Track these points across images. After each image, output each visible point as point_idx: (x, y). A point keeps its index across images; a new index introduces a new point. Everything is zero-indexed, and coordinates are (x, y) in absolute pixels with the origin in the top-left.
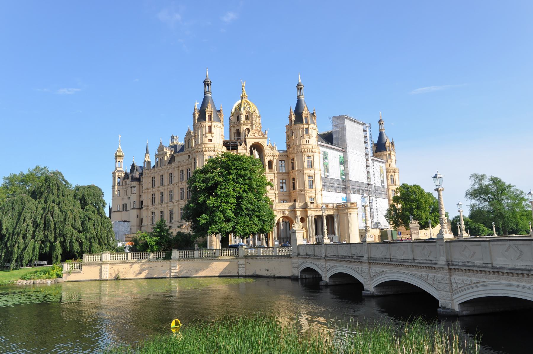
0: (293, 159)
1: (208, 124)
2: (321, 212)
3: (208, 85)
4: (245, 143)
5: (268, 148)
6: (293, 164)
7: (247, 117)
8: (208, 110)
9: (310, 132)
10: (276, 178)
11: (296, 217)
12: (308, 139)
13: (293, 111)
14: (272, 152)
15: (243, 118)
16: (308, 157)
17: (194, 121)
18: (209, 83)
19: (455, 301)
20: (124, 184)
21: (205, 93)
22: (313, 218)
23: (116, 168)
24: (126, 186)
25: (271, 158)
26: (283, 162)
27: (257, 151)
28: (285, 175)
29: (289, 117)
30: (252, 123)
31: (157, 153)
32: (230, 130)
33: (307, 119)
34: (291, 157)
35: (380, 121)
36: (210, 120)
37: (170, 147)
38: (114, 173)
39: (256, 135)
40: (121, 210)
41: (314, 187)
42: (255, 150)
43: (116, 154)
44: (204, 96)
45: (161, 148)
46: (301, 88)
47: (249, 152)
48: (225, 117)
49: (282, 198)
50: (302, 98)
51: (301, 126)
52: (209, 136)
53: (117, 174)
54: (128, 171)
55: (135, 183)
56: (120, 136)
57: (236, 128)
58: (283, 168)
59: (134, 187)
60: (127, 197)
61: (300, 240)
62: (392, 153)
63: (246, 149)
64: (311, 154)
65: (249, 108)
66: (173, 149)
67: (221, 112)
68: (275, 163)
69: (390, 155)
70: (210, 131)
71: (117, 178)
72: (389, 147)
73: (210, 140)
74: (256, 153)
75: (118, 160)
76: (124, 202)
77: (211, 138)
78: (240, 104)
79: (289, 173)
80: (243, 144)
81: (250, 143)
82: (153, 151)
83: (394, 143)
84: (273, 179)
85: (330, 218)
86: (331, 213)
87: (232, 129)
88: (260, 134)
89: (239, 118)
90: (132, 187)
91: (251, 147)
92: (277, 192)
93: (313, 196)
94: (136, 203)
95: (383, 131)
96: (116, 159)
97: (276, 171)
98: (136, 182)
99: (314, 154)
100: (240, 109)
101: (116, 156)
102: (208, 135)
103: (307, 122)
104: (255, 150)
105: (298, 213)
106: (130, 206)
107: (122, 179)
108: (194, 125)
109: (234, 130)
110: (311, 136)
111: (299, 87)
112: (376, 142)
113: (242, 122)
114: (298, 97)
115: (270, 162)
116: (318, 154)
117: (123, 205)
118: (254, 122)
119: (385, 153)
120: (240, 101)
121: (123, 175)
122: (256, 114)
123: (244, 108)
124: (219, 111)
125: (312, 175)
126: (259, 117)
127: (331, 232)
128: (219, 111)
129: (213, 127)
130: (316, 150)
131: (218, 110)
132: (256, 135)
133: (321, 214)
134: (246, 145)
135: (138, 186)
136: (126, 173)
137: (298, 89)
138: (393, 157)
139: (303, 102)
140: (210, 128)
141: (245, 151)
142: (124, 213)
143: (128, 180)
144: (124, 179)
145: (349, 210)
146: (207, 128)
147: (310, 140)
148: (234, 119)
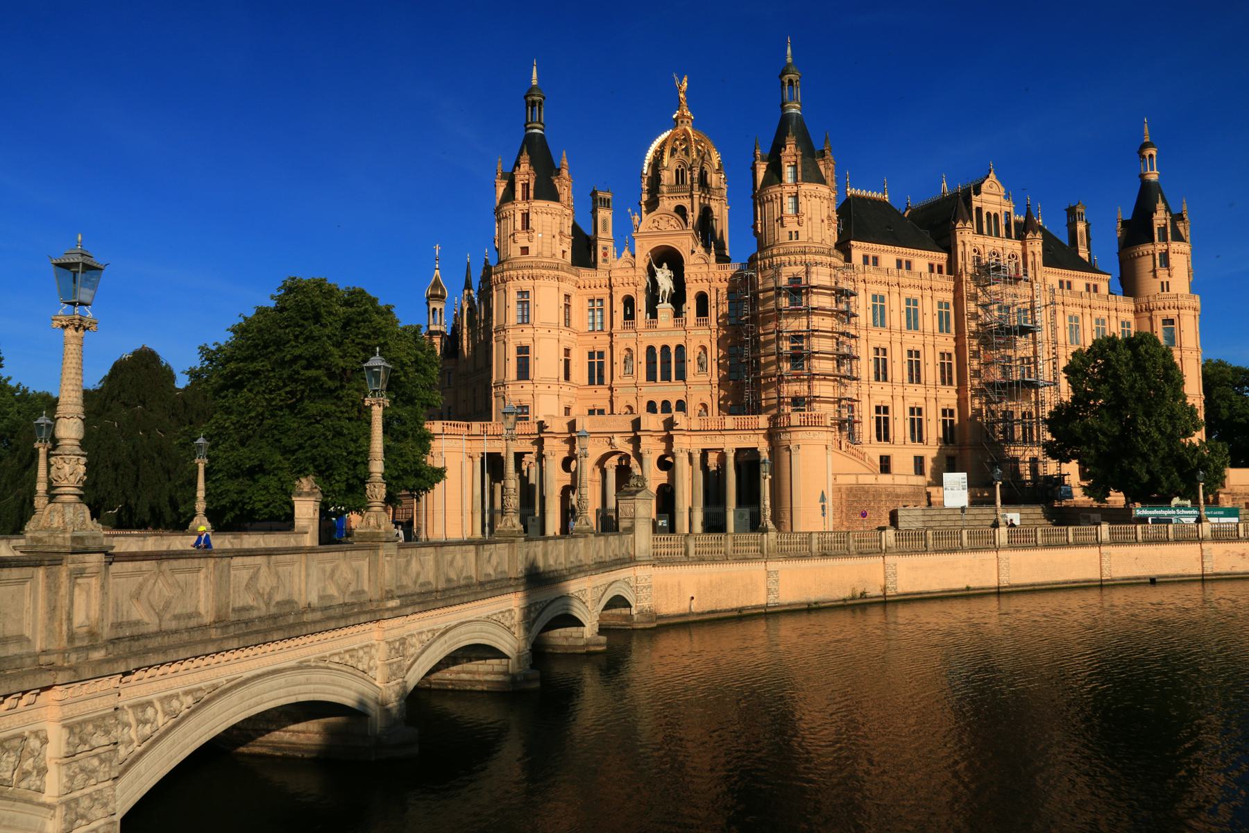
1: (520, 206)
14: (705, 268)
25: (704, 287)
36: (526, 197)
42: (665, 265)
52: (522, 240)
56: (437, 248)
70: (526, 225)
73: (525, 250)
74: (665, 279)
84: (708, 346)
102: (518, 236)
104: (665, 265)
115: (702, 299)
119: (1148, 248)
123: (673, 151)
132: (663, 225)
134: (634, 256)
140: (526, 217)
141: (631, 272)
145: (794, 435)
146: (519, 217)
147: (803, 232)
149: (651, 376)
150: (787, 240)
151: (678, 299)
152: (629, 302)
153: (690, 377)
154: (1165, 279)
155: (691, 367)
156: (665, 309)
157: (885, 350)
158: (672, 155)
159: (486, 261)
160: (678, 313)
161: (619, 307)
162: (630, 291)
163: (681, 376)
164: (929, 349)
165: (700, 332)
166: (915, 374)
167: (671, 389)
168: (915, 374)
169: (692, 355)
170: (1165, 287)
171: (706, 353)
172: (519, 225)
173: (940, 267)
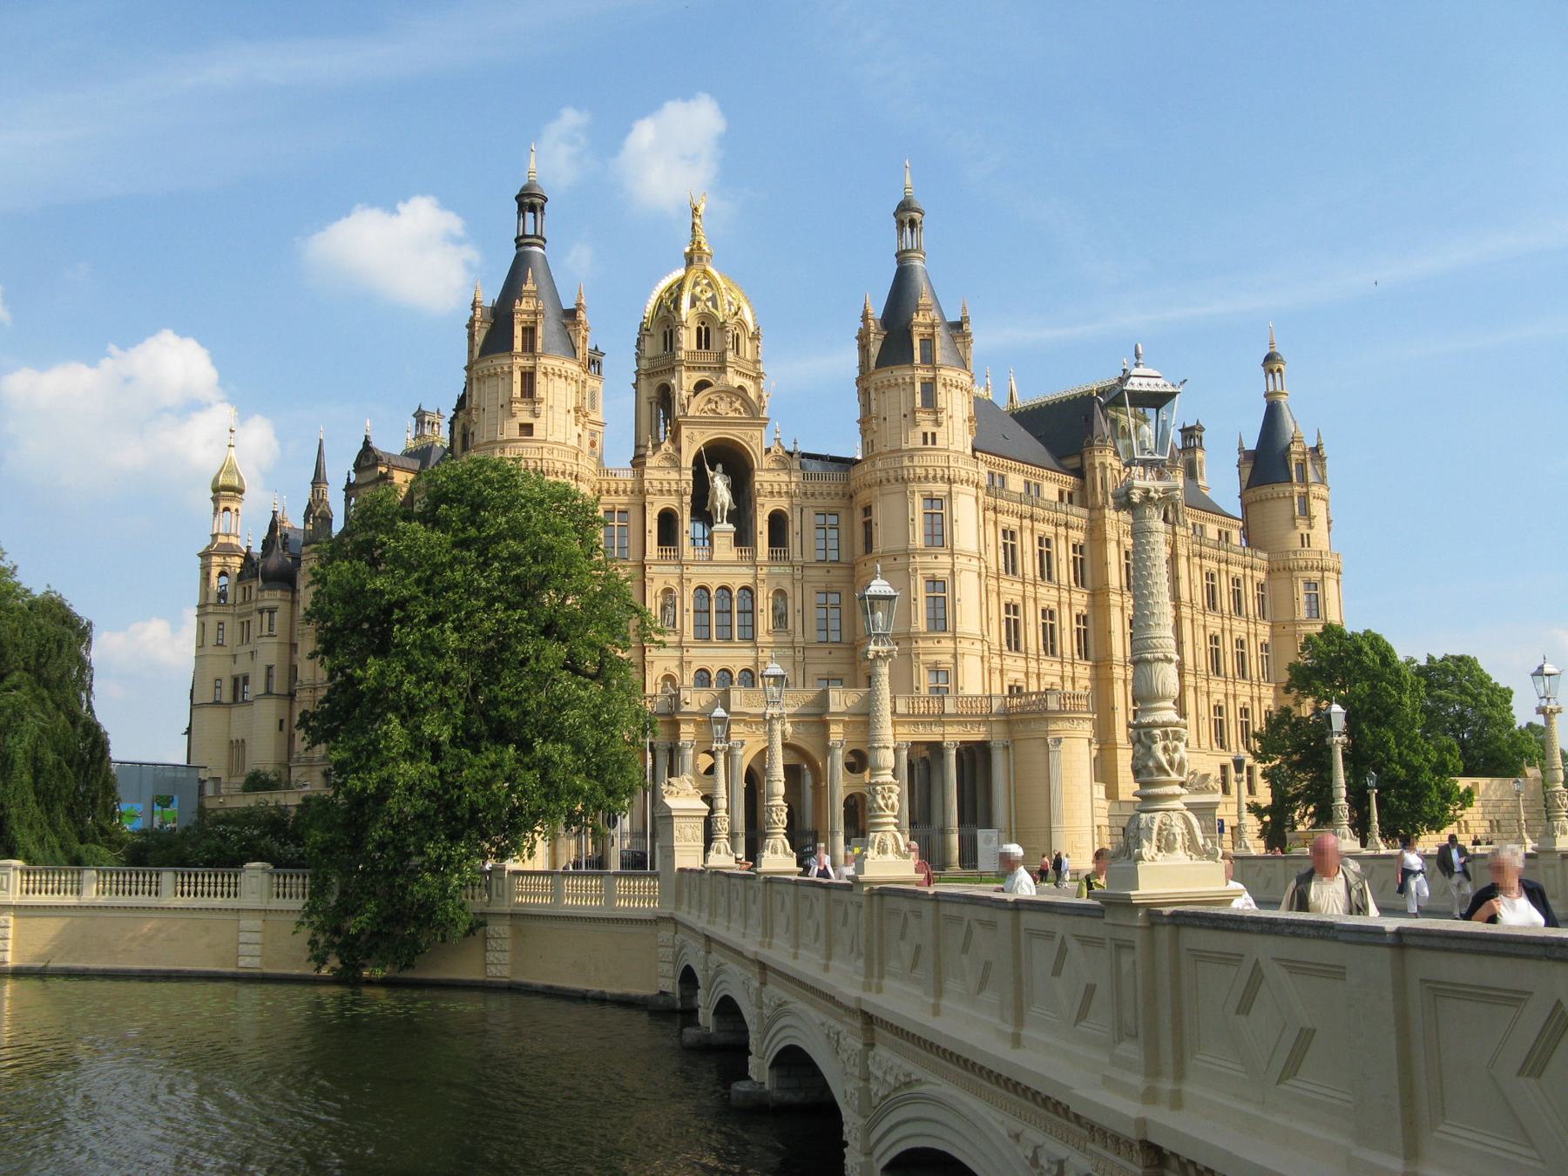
0: (867, 510)
2: (937, 730)
3: (533, 208)
4: (675, 438)
5: (767, 462)
6: (868, 526)
7: (704, 339)
8: (524, 306)
9: (941, 403)
10: (798, 585)
11: (827, 750)
12: (930, 429)
13: (877, 311)
15: (687, 340)
16: (930, 499)
17: (471, 351)
18: (537, 201)
19: (877, 1153)
20: (239, 600)
21: (520, 241)
22: (905, 753)
23: (215, 536)
24: (245, 609)
26: (832, 520)
27: (724, 472)
28: (838, 573)
29: (859, 338)
30: (722, 357)
31: (353, 478)
32: (635, 386)
33: (928, 343)
34: (863, 497)
35: (1270, 359)
37: (409, 454)
38: (205, 555)
39: (723, 408)
40: (227, 697)
41: (950, 627)
42: (719, 467)
43: (216, 480)
44: (514, 252)
45: (367, 457)
46: (913, 223)
47: (688, 475)
48: (615, 334)
49: (823, 670)
50: (918, 263)
51: (900, 373)
53: (216, 560)
54: (257, 549)
55: (273, 598)
57: (657, 381)
58: (833, 544)
59: (271, 611)
60: (248, 648)
61: (687, 853)
62: (1314, 489)
63: (676, 464)
64: (939, 489)
65: (713, 299)
66: (416, 464)
67: (582, 316)
68: (794, 527)
69: (1304, 499)
71: (215, 572)
72: (1302, 466)
73: (527, 429)
75: (222, 505)
76: (239, 670)
77: (527, 419)
78: (680, 285)
79: (852, 567)
80: (667, 446)
81: (693, 441)
82: (340, 471)
83: (1325, 451)
85: (975, 758)
86: (977, 734)
87: (643, 383)
88: (737, 405)
89: (670, 340)
90: (261, 611)
91: (698, 461)
92: (799, 639)
93: (946, 659)
94: (275, 672)
95: (1283, 400)
96: (215, 500)
97: (797, 557)
98: (279, 594)
99: (956, 487)
100: (677, 302)
101: (216, 490)
102: (516, 406)
103: (929, 359)
104: (719, 467)
105: (836, 733)
106: (257, 686)
107: (234, 579)
108: (468, 369)
109: (649, 390)
110: (943, 417)
111: (906, 216)
112: (1251, 444)
113: (682, 355)
114: (902, 256)
115: (778, 522)
116: (972, 490)
117: (236, 680)
118: (730, 356)
120: (680, 273)
121: (237, 562)
122: (742, 324)
124: (571, 314)
125: (942, 574)
126: (755, 337)
127: (976, 811)
128: (571, 314)
129: (539, 377)
130: (963, 475)
131: (568, 305)
133: (938, 738)
134: (679, 450)
135: (283, 609)
136: (248, 557)
137: (901, 224)
138: (1317, 508)
139: (920, 278)
140: (529, 378)
141: (674, 475)
142: (237, 711)
143: (254, 585)
144: (240, 577)
145: (1052, 727)
146: (517, 377)
148: (653, 347)
149: (703, 635)
150: (921, 445)
151: (741, 516)
152: (668, 521)
153: (763, 637)
154: (1305, 531)
155: (764, 621)
156: (724, 529)
157: (1051, 612)
158: (693, 304)
159: (366, 442)
160: (743, 538)
161: (652, 525)
162: (671, 502)
163: (750, 636)
164: (1030, 604)
165: (776, 570)
166: (1050, 644)
167: (711, 652)
168: (1050, 644)
169: (764, 601)
170: (1305, 540)
171: (753, 601)
172: (517, 390)
173: (1070, 495)
